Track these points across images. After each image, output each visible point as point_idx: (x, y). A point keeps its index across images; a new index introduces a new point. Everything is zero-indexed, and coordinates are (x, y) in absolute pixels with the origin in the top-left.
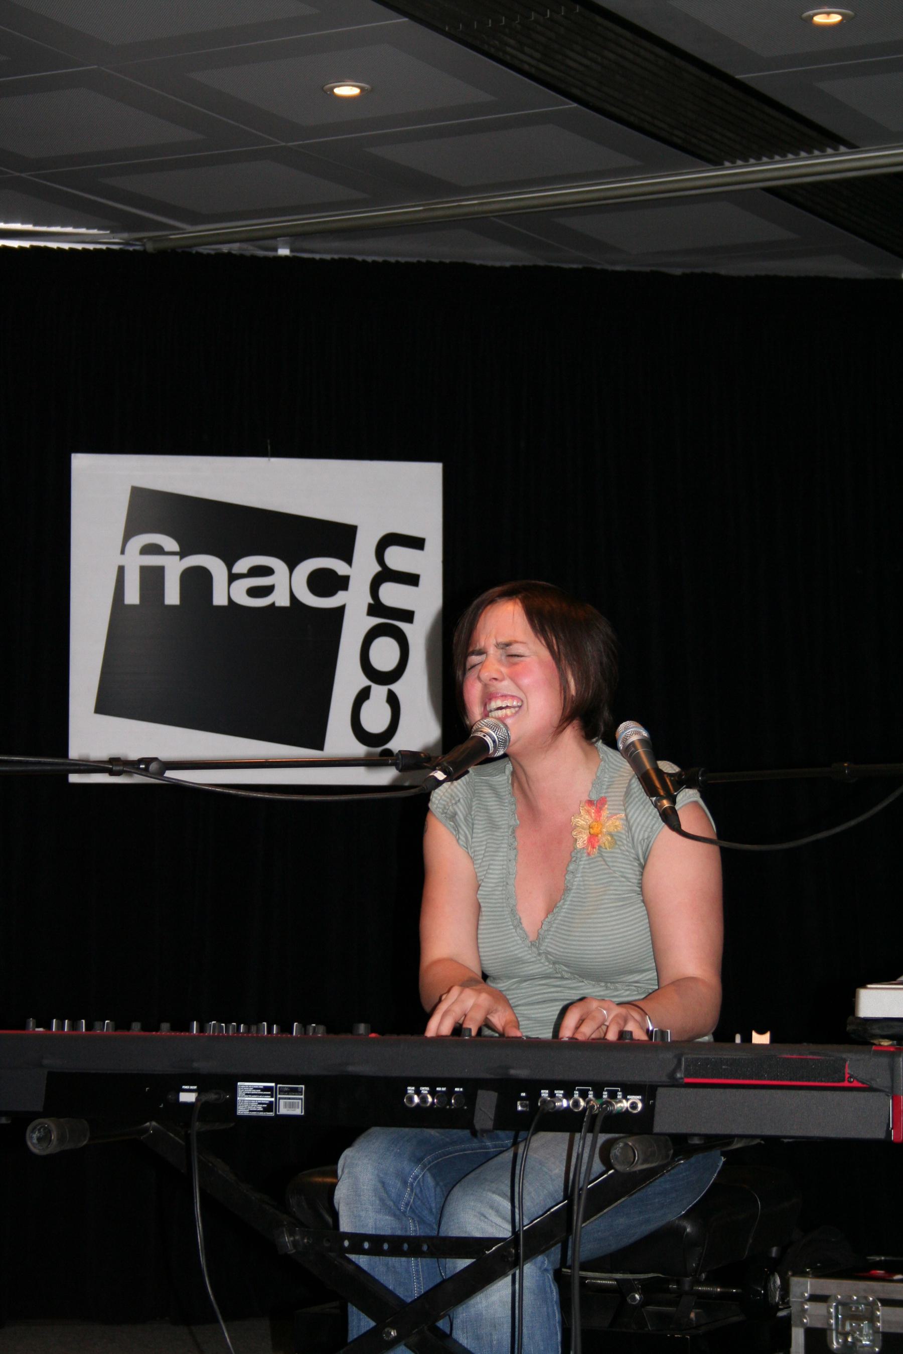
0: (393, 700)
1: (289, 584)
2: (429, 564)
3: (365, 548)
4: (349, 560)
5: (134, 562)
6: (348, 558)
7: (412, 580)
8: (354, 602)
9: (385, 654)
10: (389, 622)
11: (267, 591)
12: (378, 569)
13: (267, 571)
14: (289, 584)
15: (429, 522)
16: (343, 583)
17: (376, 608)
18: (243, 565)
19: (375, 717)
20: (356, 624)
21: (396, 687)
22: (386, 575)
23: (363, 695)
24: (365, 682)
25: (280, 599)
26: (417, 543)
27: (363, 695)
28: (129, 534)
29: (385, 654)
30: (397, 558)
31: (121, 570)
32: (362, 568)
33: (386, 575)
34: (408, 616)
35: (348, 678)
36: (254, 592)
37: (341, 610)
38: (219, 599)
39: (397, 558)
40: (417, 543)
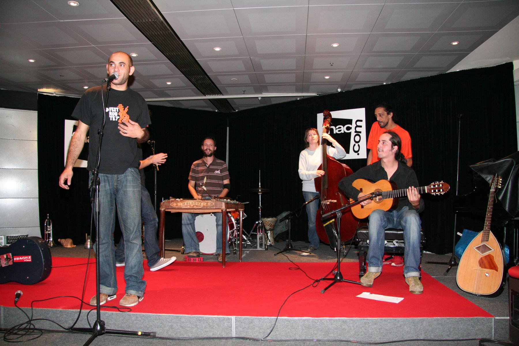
0: (359, 146)
1: (343, 129)
2: (363, 124)
4: (351, 124)
6: (351, 124)
7: (361, 127)
8: (352, 131)
9: (357, 138)
11: (340, 131)
13: (340, 128)
14: (343, 129)
15: (363, 118)
16: (351, 128)
17: (356, 132)
18: (337, 127)
20: (353, 134)
22: (357, 126)
23: (355, 145)
25: (342, 132)
26: (361, 121)
27: (355, 145)
30: (359, 124)
32: (353, 126)
33: (357, 126)
34: (360, 132)
35: (352, 143)
36: (339, 131)
37: (350, 133)
38: (335, 133)
39: (359, 124)
40: (361, 121)
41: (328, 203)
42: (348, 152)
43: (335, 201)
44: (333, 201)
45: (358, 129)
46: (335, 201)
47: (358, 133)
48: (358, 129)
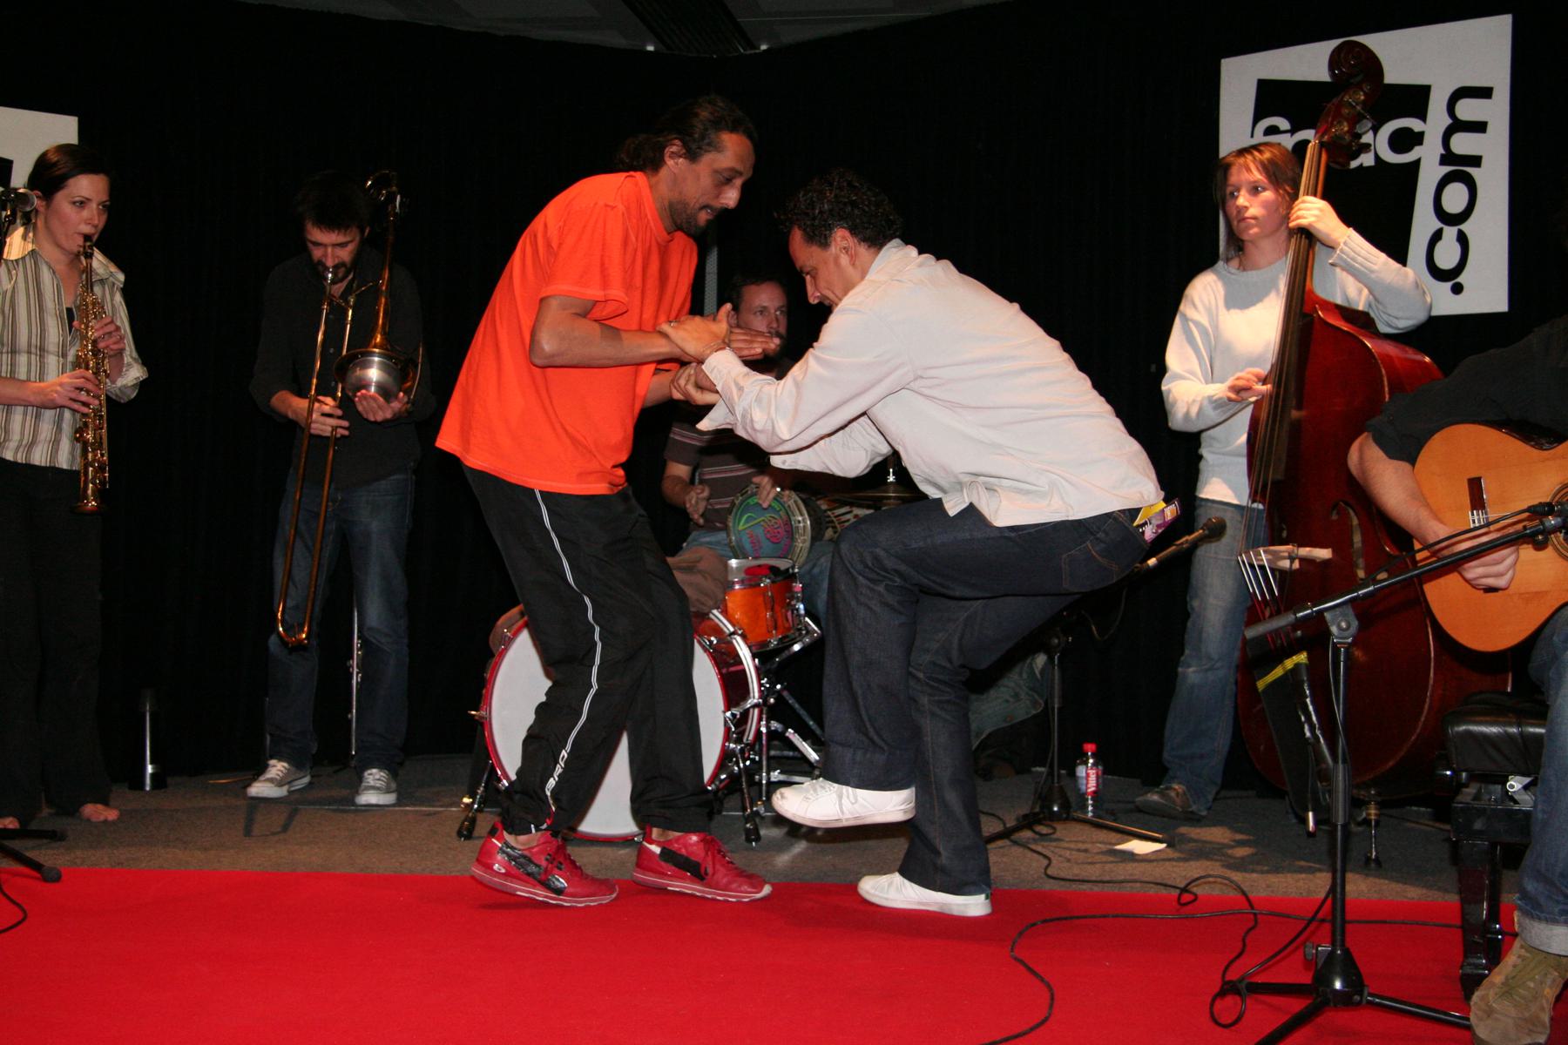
0: (1463, 239)
2: (1497, 112)
4: (1423, 118)
6: (1423, 118)
7: (1479, 127)
8: (1428, 156)
9: (1455, 198)
15: (1499, 75)
17: (1448, 158)
21: (1463, 227)
22: (1457, 126)
23: (1437, 236)
24: (1439, 225)
26: (1485, 93)
27: (1437, 236)
28: (1256, 120)
30: (1468, 110)
32: (1436, 121)
34: (1476, 161)
35: (1423, 221)
37: (1417, 163)
39: (1468, 110)
40: (1485, 93)
41: (1286, 564)
43: (1324, 554)
44: (1304, 551)
45: (1463, 144)
46: (1324, 554)
47: (1460, 168)
48: (1463, 144)
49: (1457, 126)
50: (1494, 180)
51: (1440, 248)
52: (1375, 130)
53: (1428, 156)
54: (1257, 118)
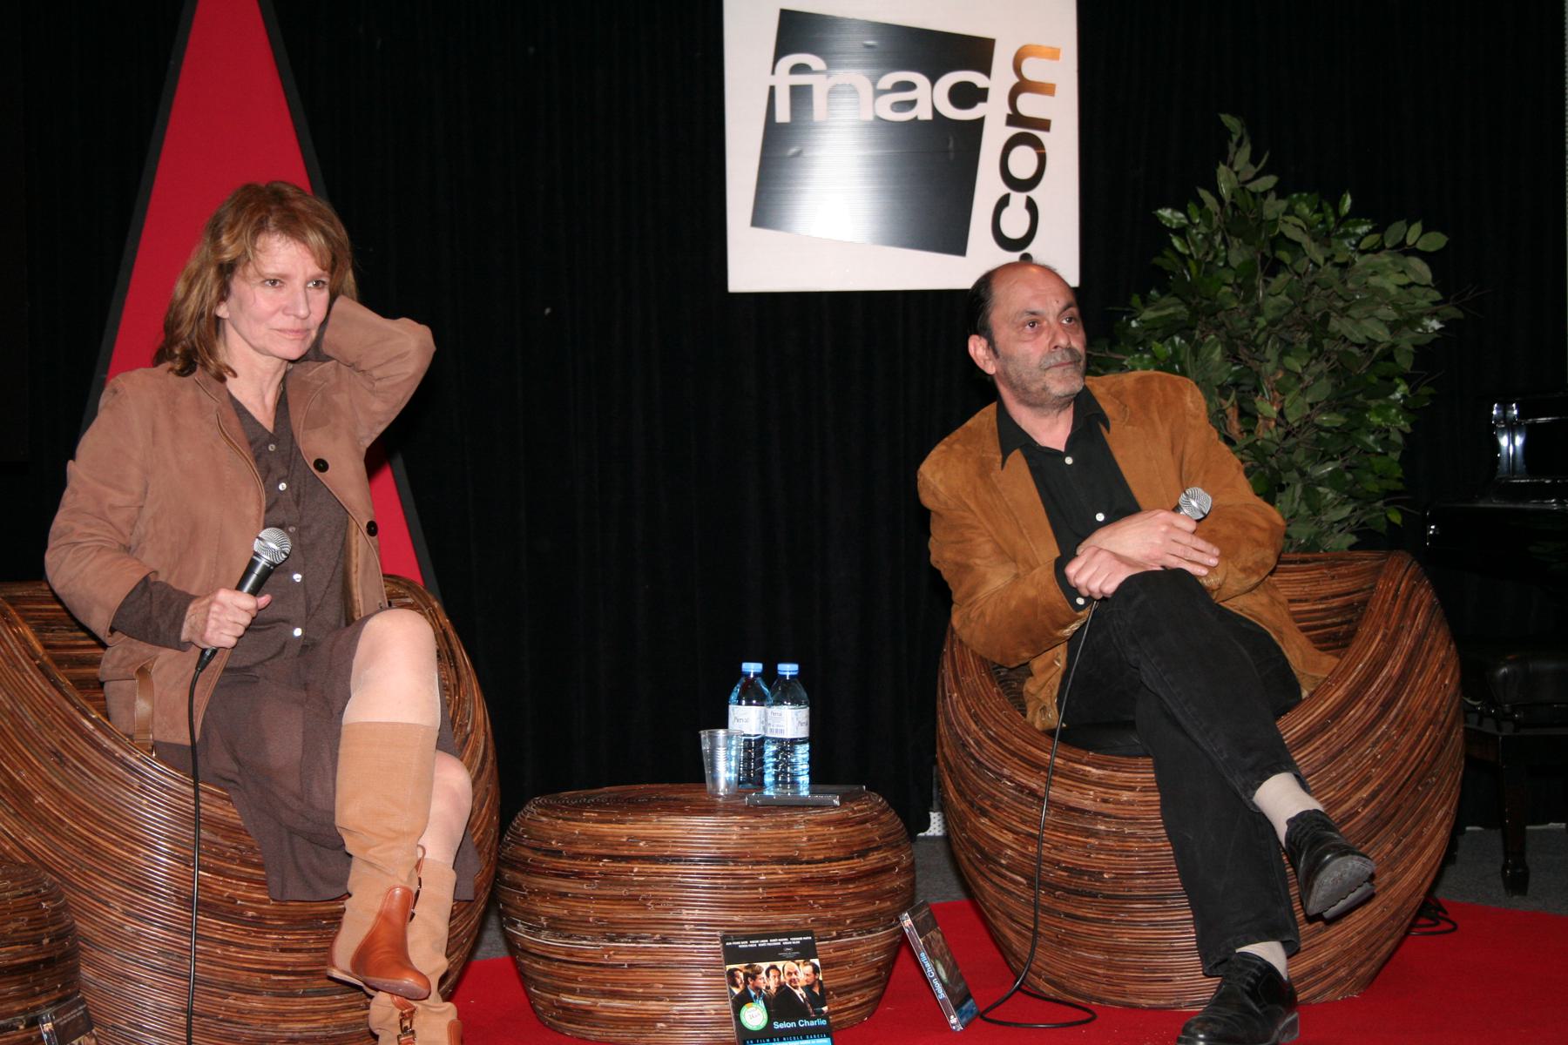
0: (1031, 206)
3: (1002, 60)
4: (986, 70)
5: (784, 81)
6: (986, 70)
7: (1045, 89)
8: (993, 113)
9: (1023, 162)
10: (1027, 131)
11: (913, 104)
12: (1015, 80)
13: (910, 86)
17: (1015, 119)
19: (1015, 224)
21: (1033, 194)
23: (1004, 202)
24: (1006, 190)
26: (1054, 54)
27: (1004, 202)
29: (1023, 162)
30: (1031, 70)
31: (772, 89)
32: (999, 81)
34: (1044, 125)
35: (988, 185)
37: (979, 123)
40: (1054, 54)
42: (955, 243)
47: (1027, 131)
48: (1029, 105)
49: (1022, 86)
50: (1063, 143)
51: (1006, 214)
52: (933, 81)
53: (993, 113)
54: (781, 50)
